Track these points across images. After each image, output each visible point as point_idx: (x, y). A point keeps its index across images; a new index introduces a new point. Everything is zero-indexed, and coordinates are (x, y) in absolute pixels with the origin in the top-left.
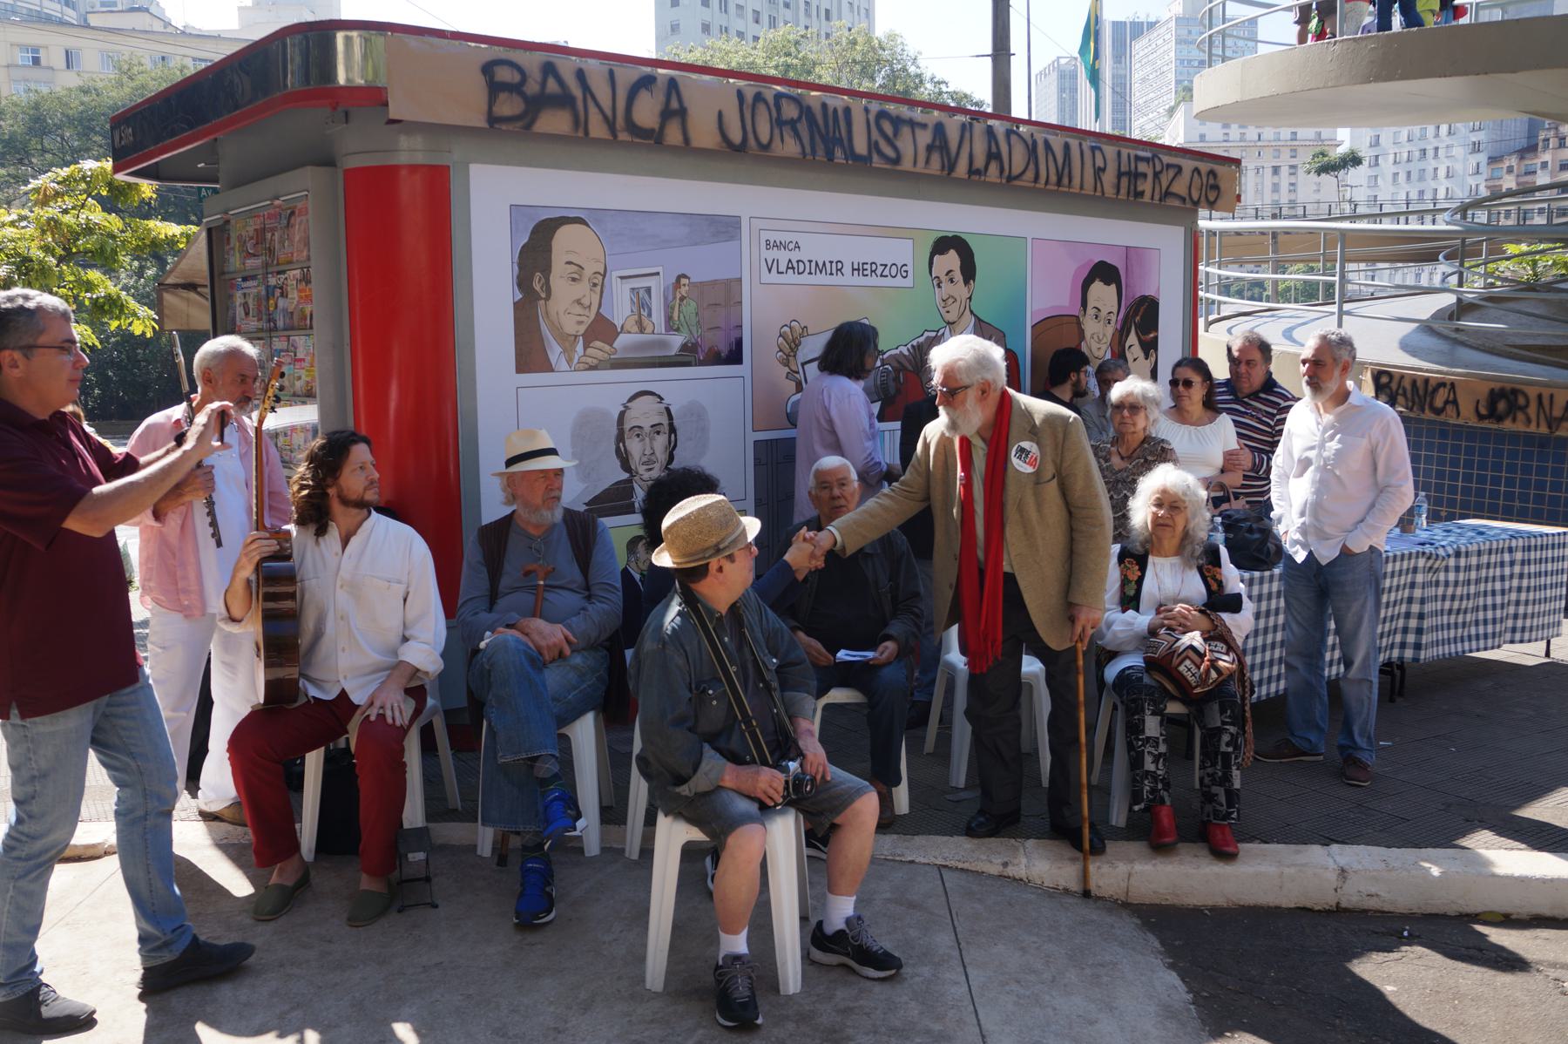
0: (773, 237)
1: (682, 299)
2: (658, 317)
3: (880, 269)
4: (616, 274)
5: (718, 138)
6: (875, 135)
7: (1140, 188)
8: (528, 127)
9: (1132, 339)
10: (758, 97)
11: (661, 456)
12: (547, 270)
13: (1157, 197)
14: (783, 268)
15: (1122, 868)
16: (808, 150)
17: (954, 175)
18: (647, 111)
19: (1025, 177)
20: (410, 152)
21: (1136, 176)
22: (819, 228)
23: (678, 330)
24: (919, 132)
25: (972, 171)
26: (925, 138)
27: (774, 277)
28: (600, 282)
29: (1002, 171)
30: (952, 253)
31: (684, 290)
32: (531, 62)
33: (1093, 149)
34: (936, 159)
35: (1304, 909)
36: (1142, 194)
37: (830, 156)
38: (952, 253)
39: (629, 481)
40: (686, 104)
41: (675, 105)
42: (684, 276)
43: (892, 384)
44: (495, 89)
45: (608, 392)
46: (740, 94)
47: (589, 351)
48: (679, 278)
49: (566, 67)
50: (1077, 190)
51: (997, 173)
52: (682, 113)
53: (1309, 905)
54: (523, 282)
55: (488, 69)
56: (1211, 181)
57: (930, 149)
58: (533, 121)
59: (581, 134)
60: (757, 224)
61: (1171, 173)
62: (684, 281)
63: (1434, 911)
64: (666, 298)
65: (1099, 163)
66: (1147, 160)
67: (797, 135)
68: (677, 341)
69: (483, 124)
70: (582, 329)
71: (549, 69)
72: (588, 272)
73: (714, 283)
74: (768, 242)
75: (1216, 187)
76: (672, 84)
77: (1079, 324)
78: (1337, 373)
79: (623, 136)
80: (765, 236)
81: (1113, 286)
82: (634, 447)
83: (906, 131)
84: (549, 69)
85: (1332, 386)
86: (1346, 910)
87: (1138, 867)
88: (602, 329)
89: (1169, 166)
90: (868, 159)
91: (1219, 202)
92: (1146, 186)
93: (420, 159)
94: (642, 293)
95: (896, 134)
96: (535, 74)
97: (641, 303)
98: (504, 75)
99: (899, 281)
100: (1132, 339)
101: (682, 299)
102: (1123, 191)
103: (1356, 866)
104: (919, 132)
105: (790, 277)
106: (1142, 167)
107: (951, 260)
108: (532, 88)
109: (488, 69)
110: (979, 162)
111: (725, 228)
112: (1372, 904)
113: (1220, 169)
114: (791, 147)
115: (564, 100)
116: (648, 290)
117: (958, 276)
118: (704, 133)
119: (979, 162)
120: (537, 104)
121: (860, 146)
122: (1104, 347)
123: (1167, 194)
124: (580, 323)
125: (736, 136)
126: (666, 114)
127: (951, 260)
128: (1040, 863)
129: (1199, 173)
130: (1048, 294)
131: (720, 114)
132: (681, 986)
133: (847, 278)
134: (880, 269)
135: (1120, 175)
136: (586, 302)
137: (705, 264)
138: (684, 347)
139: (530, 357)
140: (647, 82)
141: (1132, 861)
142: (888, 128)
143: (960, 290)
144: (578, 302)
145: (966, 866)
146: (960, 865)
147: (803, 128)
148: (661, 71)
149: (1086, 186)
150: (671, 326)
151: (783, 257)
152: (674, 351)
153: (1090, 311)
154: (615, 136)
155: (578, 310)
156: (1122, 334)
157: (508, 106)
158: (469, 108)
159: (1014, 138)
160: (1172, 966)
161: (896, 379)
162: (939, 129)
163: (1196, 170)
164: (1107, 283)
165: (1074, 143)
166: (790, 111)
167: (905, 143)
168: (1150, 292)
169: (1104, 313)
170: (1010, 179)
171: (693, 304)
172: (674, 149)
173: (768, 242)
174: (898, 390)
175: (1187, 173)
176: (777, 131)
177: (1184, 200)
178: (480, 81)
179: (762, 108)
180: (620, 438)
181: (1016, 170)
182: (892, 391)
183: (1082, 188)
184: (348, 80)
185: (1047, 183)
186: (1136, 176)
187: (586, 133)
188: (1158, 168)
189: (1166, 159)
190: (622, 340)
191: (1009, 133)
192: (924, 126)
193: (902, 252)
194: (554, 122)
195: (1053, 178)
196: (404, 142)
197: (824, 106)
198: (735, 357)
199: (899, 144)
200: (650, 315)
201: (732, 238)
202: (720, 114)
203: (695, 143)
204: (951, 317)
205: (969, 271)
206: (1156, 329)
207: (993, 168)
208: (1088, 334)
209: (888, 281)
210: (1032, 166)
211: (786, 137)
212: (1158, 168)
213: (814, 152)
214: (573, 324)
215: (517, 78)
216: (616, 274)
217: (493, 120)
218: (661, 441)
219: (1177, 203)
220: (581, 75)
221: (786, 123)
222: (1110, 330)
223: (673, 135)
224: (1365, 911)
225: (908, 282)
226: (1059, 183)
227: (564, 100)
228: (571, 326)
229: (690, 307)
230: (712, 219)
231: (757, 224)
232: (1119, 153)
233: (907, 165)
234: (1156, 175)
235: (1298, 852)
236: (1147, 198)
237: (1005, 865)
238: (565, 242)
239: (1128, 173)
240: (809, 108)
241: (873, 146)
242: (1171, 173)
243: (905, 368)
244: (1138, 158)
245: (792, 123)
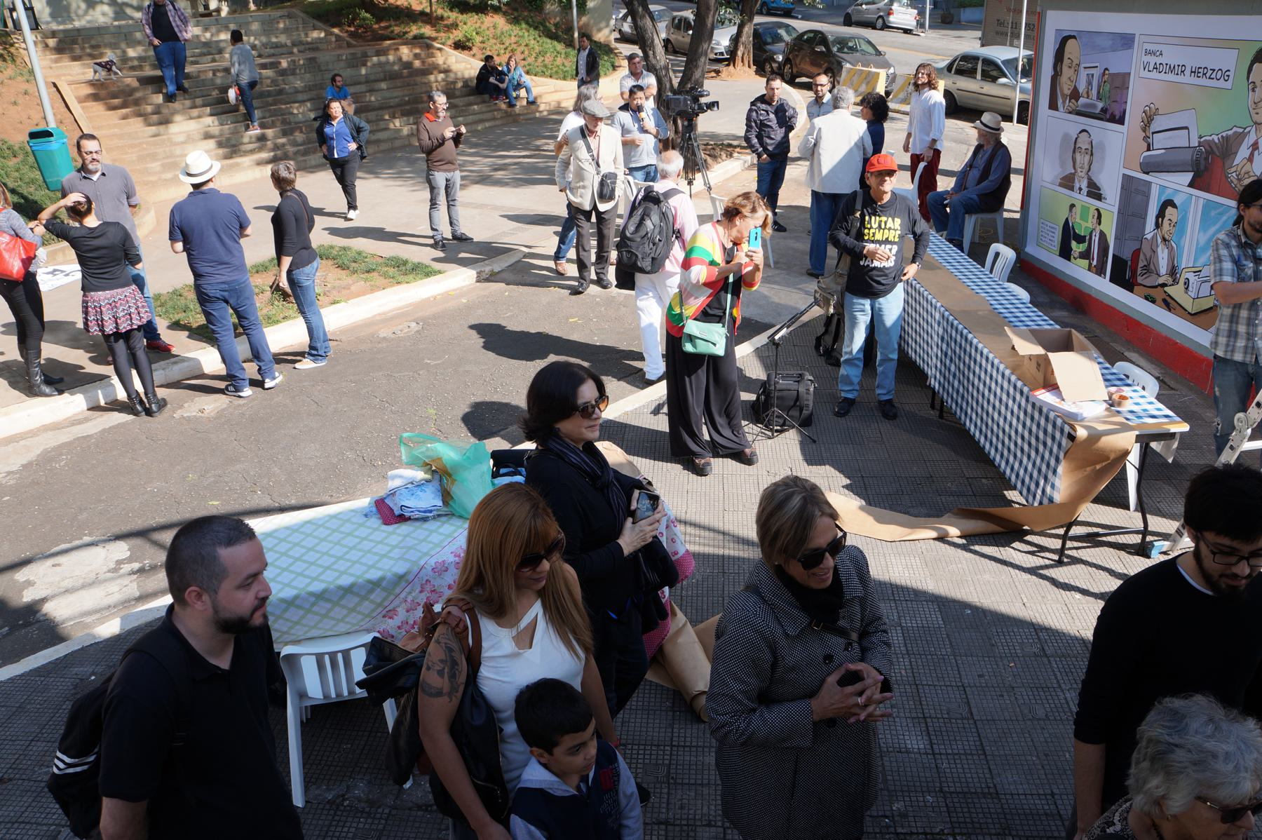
2: (1094, 92)
11: (1086, 167)
12: (1062, 62)
22: (1176, 41)
27: (1145, 74)
39: (1074, 174)
43: (1203, 162)
45: (1074, 124)
68: (1100, 105)
73: (1118, 74)
82: (1078, 156)
88: (1075, 95)
97: (1090, 84)
99: (1221, 84)
105: (1155, 75)
111: (1126, 41)
139: (1053, 105)
150: (1099, 98)
151: (1153, 60)
152: (1098, 111)
161: (1206, 159)
174: (1206, 168)
180: (1074, 152)
182: (1202, 167)
190: (1082, 100)
198: (1121, 121)
214: (1067, 92)
218: (1087, 157)
225: (1228, 85)
229: (1107, 87)
243: (1212, 152)
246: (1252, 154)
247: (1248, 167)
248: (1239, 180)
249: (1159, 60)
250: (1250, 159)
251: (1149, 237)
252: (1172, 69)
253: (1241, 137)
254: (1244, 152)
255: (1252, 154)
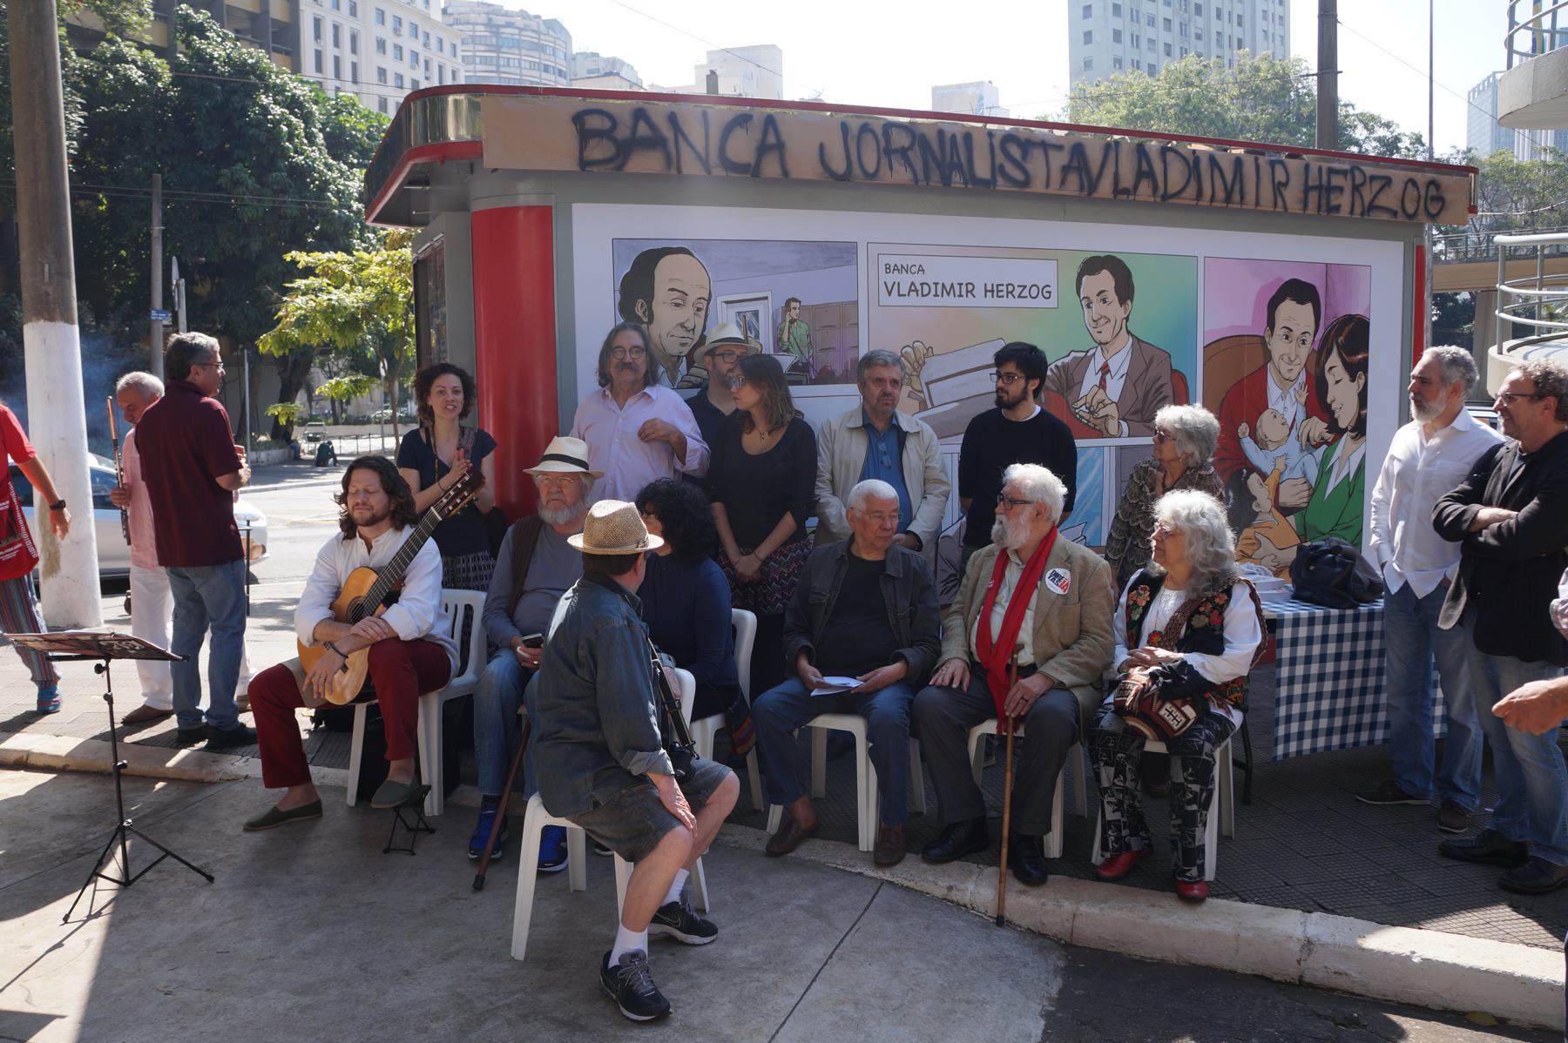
0: (892, 261)
1: (792, 321)
3: (1017, 291)
4: (720, 299)
5: (820, 169)
6: (1000, 158)
7: (1334, 203)
8: (620, 168)
9: (1334, 359)
10: (865, 128)
12: (649, 296)
13: (1358, 210)
14: (904, 290)
15: (1068, 906)
16: (921, 175)
17: (1095, 195)
18: (742, 147)
19: (1184, 195)
20: (527, 196)
21: (1326, 190)
23: (787, 350)
24: (1053, 154)
25: (1117, 190)
26: (1059, 160)
28: (704, 306)
29: (1155, 189)
30: (1105, 273)
31: (794, 313)
32: (621, 108)
33: (1272, 164)
34: (1073, 179)
35: (1262, 978)
36: (1338, 208)
37: (946, 181)
38: (1105, 273)
40: (784, 138)
41: (771, 139)
42: (795, 300)
44: (585, 135)
46: (845, 128)
47: (693, 370)
48: (788, 302)
49: (658, 112)
50: (1252, 207)
51: (1150, 191)
52: (780, 147)
53: (1268, 973)
54: (625, 307)
55: (578, 119)
56: (1433, 192)
57: (1065, 170)
58: (623, 164)
59: (673, 171)
60: (874, 249)
61: (1377, 185)
62: (793, 304)
63: (1414, 1001)
64: (774, 321)
65: (1280, 176)
66: (1344, 173)
67: (908, 163)
69: (571, 164)
70: (686, 350)
71: (640, 115)
72: (692, 298)
73: (827, 306)
74: (887, 267)
75: (1440, 199)
76: (770, 122)
77: (1264, 344)
78: (1443, 394)
79: (718, 172)
80: (884, 260)
81: (1309, 307)
83: (1038, 154)
84: (640, 115)
85: (1439, 406)
86: (1310, 985)
87: (1084, 908)
89: (1373, 178)
90: (993, 181)
91: (1443, 215)
92: (1344, 200)
93: (533, 200)
94: (748, 316)
95: (1025, 156)
96: (626, 121)
97: (748, 324)
98: (594, 123)
100: (1334, 359)
101: (792, 321)
102: (1312, 206)
103: (1326, 939)
104: (1053, 154)
105: (914, 299)
106: (1337, 180)
107: (1105, 280)
108: (623, 132)
109: (578, 119)
110: (1127, 180)
111: (842, 254)
112: (1340, 982)
113: (1444, 180)
114: (901, 174)
115: (655, 142)
116: (756, 314)
117: (1112, 296)
118: (804, 163)
119: (1127, 180)
120: (625, 149)
121: (982, 170)
122: (1297, 369)
123: (1372, 207)
124: (683, 345)
125: (839, 165)
126: (763, 149)
127: (1105, 280)
128: (978, 887)
129: (1415, 184)
130: (1225, 312)
131: (822, 147)
132: (544, 955)
133: (980, 299)
134: (1017, 291)
135: (1307, 190)
136: (690, 325)
137: (817, 288)
138: (794, 367)
140: (743, 121)
141: (1078, 902)
142: (1015, 151)
143: (1115, 310)
144: (682, 325)
145: (911, 884)
146: (906, 883)
147: (915, 156)
148: (758, 109)
149: (1262, 201)
151: (905, 280)
153: (1279, 331)
154: (709, 172)
155: (682, 332)
156: (1321, 354)
157: (599, 150)
158: (561, 151)
159: (1170, 156)
160: (1047, 1016)
162: (1078, 150)
163: (1412, 181)
164: (1301, 302)
165: (1249, 162)
166: (900, 140)
167: (1036, 164)
168: (1358, 310)
169: (1297, 333)
170: (1165, 197)
171: (804, 327)
172: (772, 181)
173: (887, 267)
175: (1397, 186)
176: (884, 160)
177: (1395, 213)
178: (572, 129)
179: (868, 138)
181: (1172, 189)
183: (1257, 203)
184: (457, 136)
185: (1212, 199)
186: (1326, 190)
187: (679, 171)
188: (1359, 180)
189: (1369, 170)
191: (1164, 151)
192: (1060, 148)
193: (1044, 273)
194: (645, 162)
195: (1220, 194)
196: (522, 187)
197: (941, 133)
199: (1029, 166)
200: (757, 336)
201: (848, 263)
202: (822, 147)
203: (794, 175)
204: (1103, 338)
205: (1125, 291)
206: (1364, 347)
207: (1145, 188)
208: (1275, 355)
209: (1028, 302)
210: (1193, 183)
211: (895, 165)
212: (1359, 180)
213: (927, 178)
215: (607, 124)
216: (720, 299)
217: (584, 164)
219: (1385, 217)
220: (673, 119)
221: (896, 151)
222: (1304, 351)
223: (771, 167)
224: (1332, 990)
225: (1052, 302)
226: (1228, 199)
227: (655, 142)
228: (673, 347)
229: (801, 330)
230: (825, 246)
231: (874, 249)
232: (1307, 167)
233: (1038, 186)
234: (1356, 188)
235: (1268, 916)
236: (1344, 212)
237: (950, 888)
238: (666, 270)
239: (1319, 188)
240: (923, 136)
241: (997, 170)
242: (1377, 185)
244: (1331, 171)
245: (903, 152)
246: (1103, 380)
247: (1101, 395)
248: (1091, 413)
249: (918, 279)
250: (1102, 385)
251: (951, 532)
252: (948, 290)
253: (1083, 363)
254: (1091, 379)
255: (1103, 380)
